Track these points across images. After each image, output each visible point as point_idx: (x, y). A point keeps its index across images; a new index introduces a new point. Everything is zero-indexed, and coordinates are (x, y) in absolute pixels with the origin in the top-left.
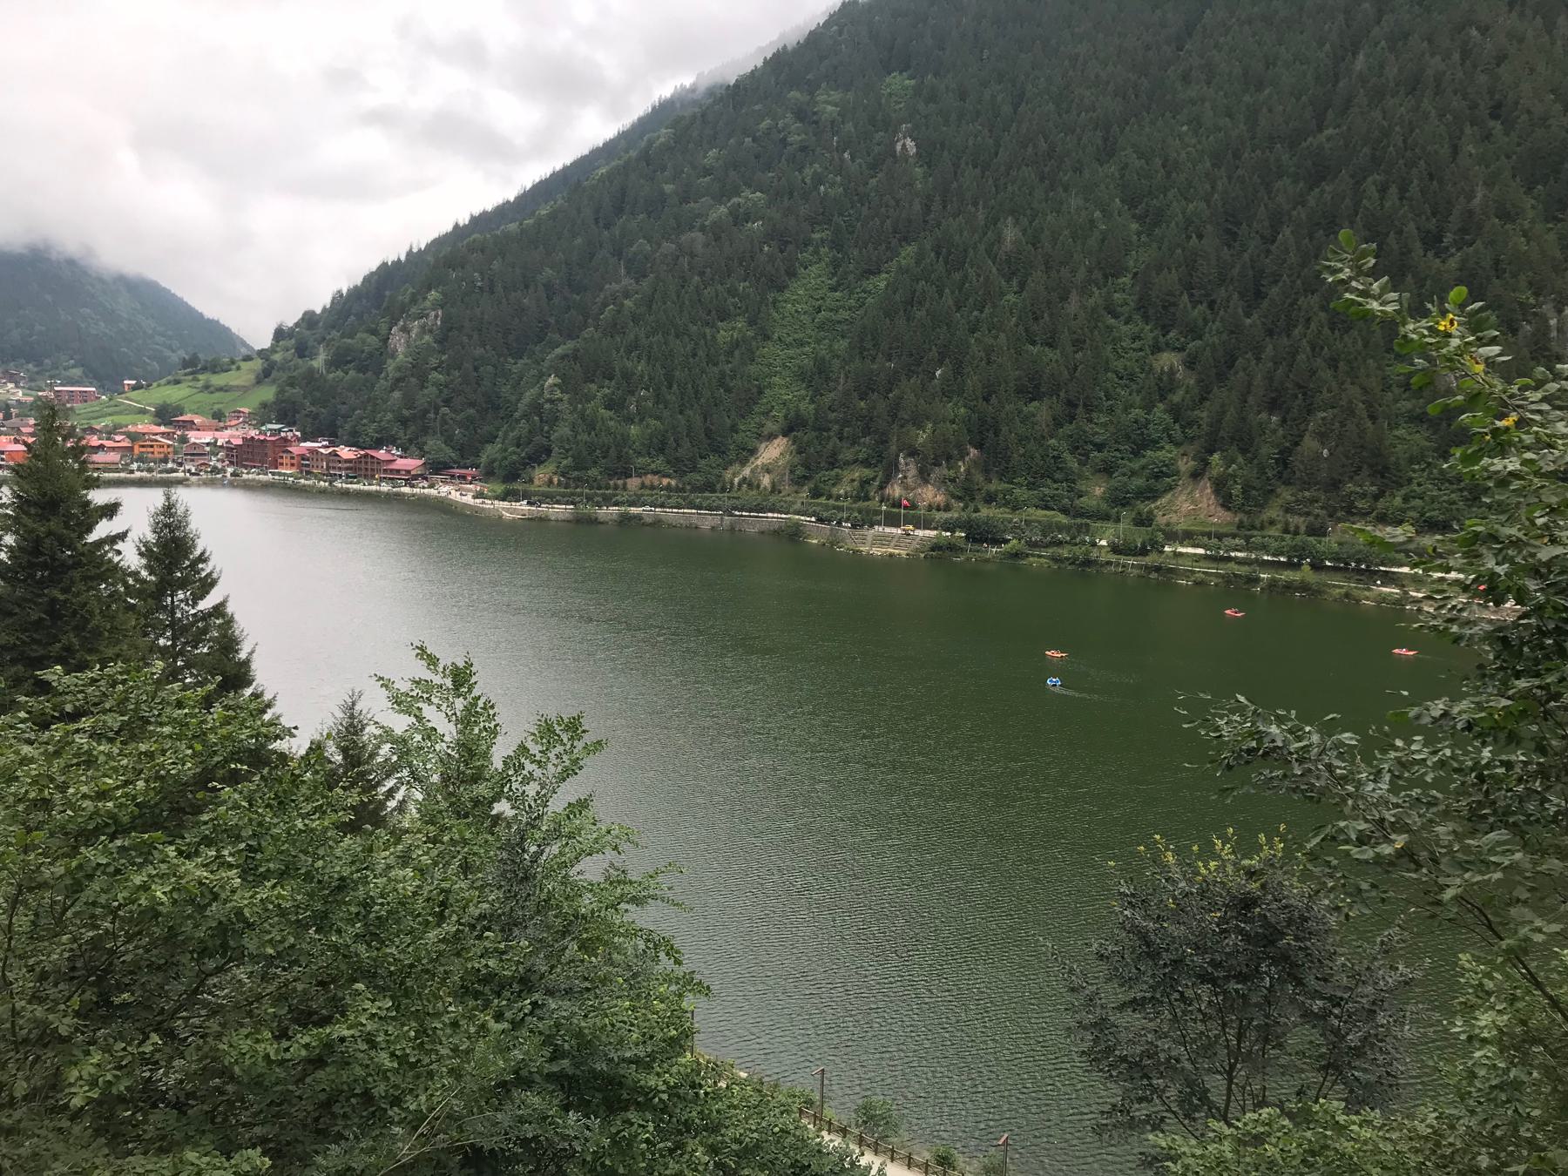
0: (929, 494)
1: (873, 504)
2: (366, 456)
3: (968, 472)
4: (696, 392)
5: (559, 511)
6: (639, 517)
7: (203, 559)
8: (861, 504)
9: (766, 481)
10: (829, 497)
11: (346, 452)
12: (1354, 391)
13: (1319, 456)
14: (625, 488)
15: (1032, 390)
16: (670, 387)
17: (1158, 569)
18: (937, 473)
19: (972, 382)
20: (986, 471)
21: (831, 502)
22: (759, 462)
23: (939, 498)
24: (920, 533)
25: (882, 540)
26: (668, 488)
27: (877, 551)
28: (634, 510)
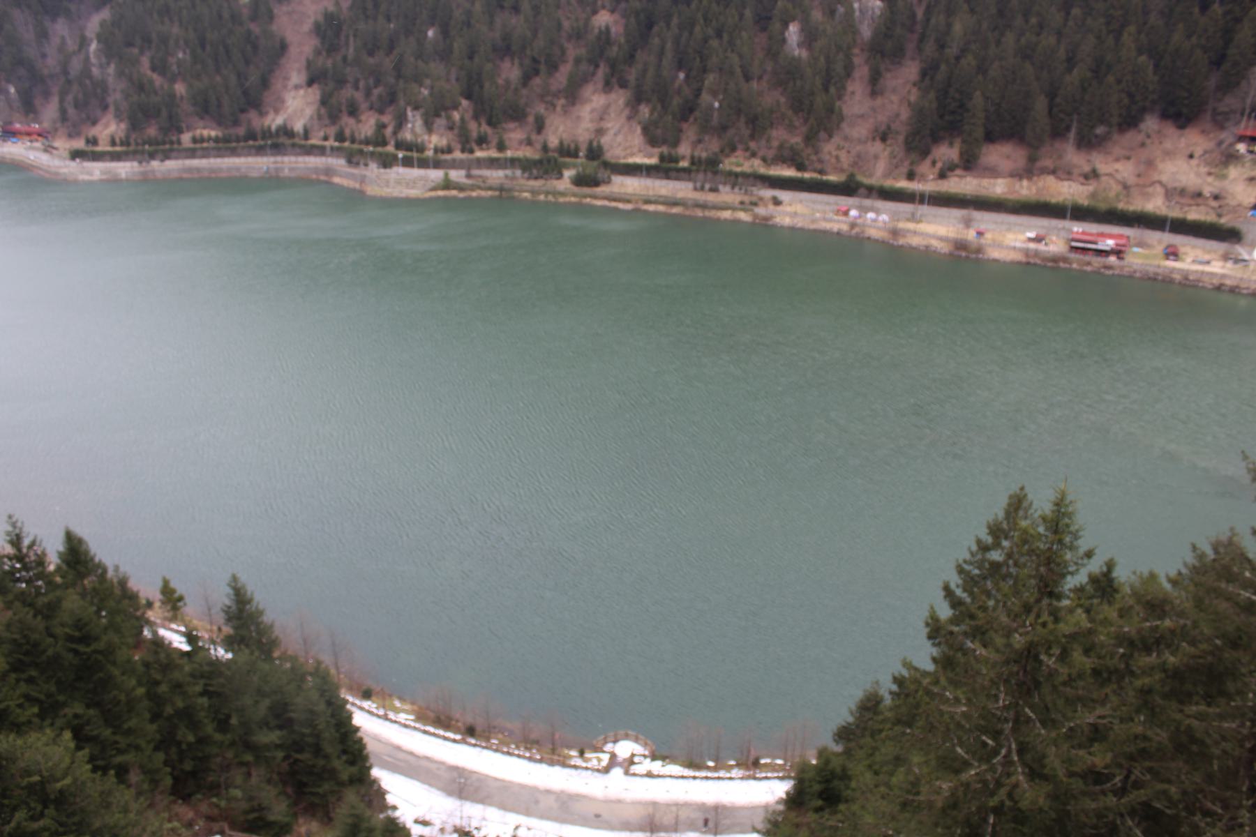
1: (390, 148)
3: (462, 119)
4: (227, 52)
5: (125, 169)
8: (380, 149)
12: (735, 59)
13: (711, 107)
14: (179, 142)
15: (505, 49)
16: (203, 47)
18: (441, 122)
19: (458, 45)
20: (476, 117)
21: (356, 146)
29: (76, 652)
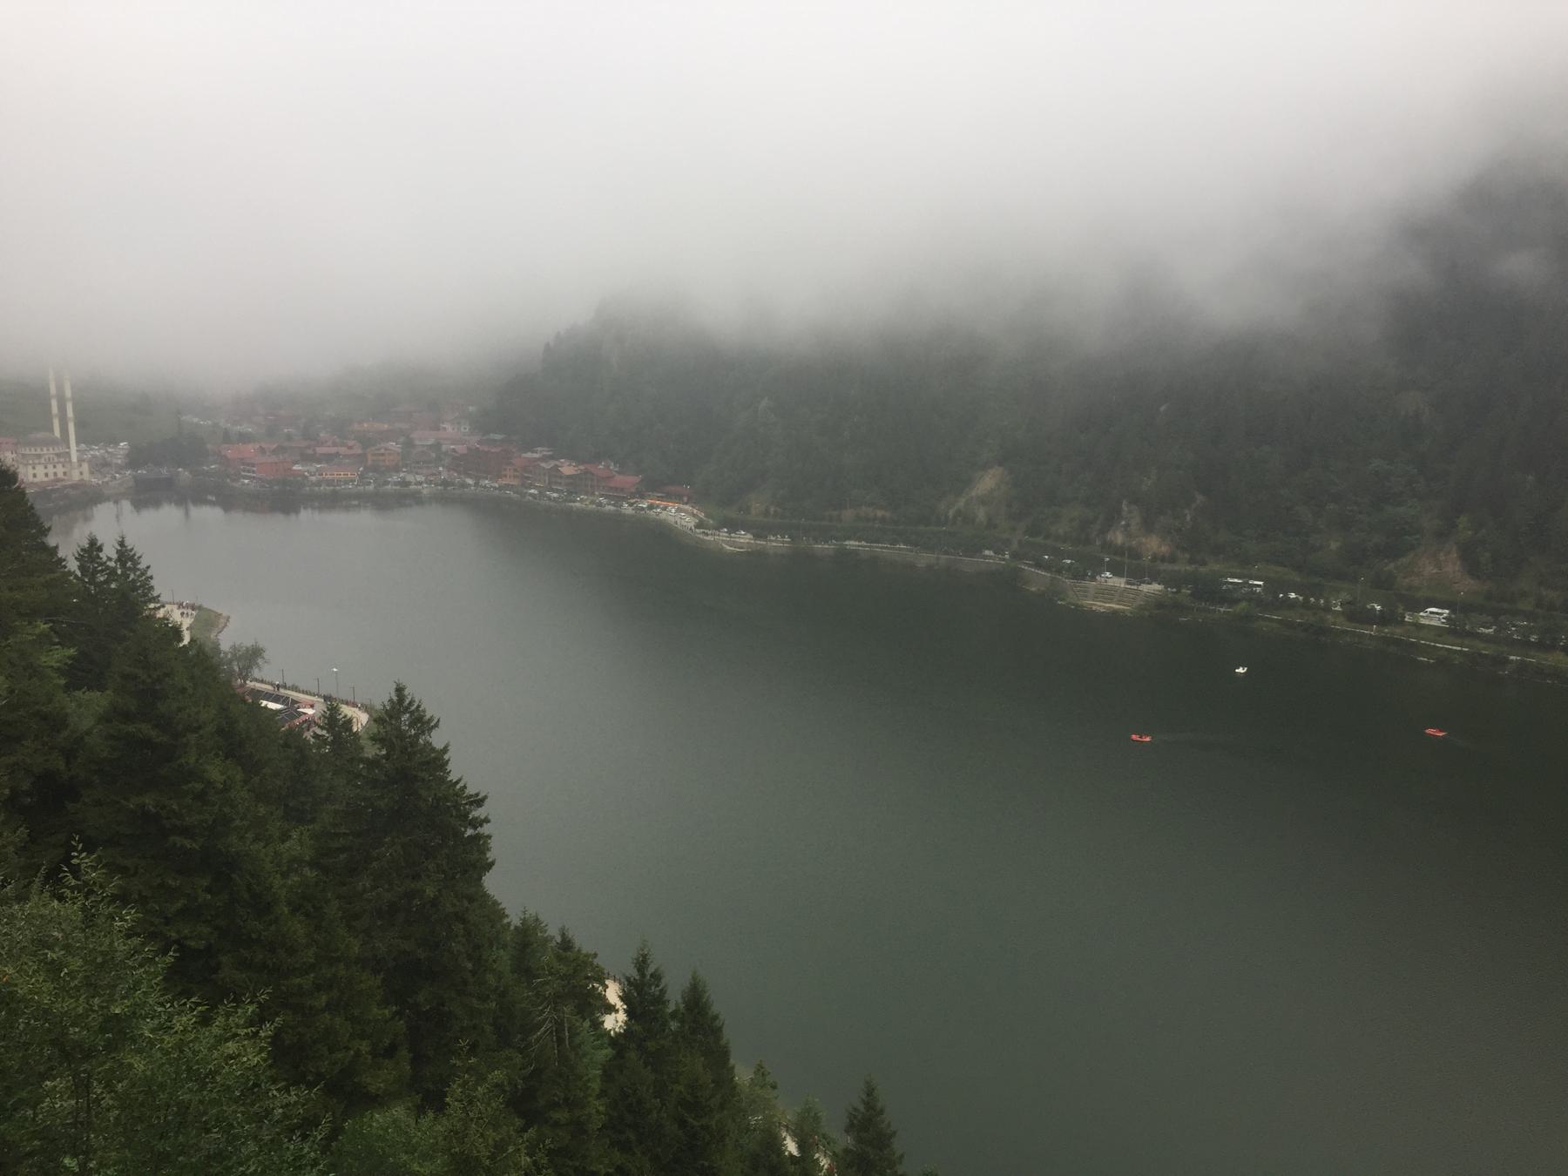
0: (1154, 545)
2: (586, 472)
6: (855, 553)
7: (716, 1017)
9: (981, 514)
10: (1047, 537)
11: (568, 469)
17: (1398, 642)
22: (974, 493)
23: (1164, 549)
24: (1145, 588)
25: (1107, 593)
26: (883, 520)
27: (1101, 606)
28: (852, 544)
29: (683, 1123)
